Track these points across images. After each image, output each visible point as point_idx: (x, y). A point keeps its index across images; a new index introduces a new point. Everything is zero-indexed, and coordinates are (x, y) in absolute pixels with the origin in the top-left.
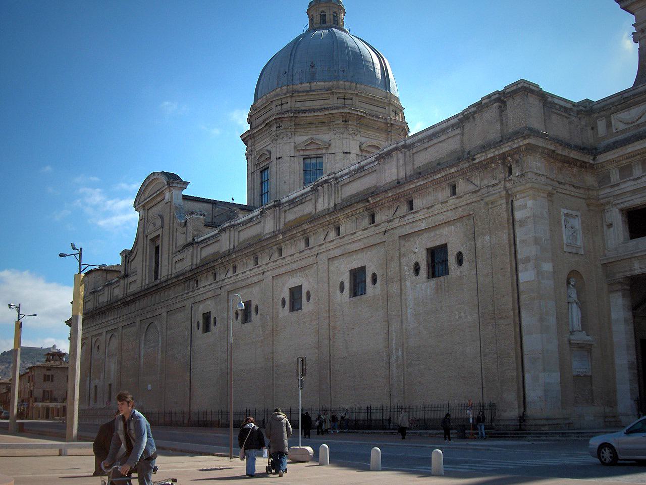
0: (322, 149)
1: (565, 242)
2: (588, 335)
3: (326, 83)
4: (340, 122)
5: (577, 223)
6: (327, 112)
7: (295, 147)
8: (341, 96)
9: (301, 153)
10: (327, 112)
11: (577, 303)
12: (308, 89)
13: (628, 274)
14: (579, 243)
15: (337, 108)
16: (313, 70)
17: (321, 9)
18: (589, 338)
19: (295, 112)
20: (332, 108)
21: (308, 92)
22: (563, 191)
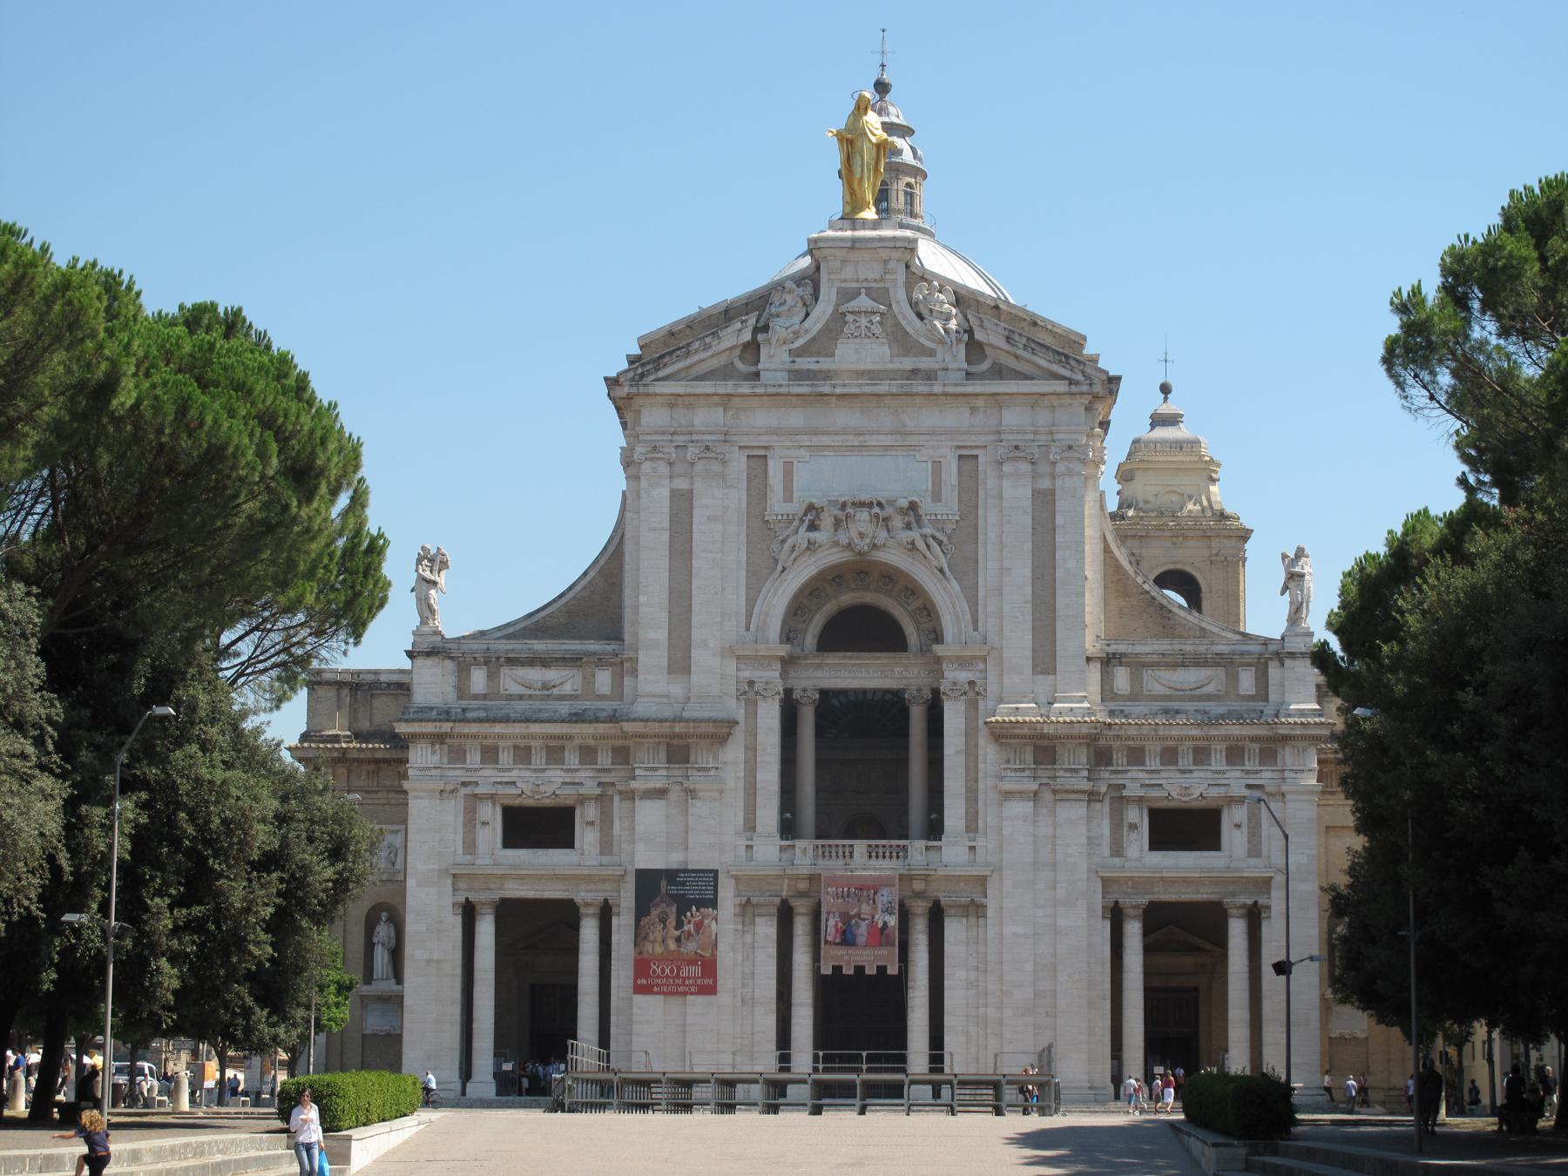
11: (383, 945)
22: (376, 802)
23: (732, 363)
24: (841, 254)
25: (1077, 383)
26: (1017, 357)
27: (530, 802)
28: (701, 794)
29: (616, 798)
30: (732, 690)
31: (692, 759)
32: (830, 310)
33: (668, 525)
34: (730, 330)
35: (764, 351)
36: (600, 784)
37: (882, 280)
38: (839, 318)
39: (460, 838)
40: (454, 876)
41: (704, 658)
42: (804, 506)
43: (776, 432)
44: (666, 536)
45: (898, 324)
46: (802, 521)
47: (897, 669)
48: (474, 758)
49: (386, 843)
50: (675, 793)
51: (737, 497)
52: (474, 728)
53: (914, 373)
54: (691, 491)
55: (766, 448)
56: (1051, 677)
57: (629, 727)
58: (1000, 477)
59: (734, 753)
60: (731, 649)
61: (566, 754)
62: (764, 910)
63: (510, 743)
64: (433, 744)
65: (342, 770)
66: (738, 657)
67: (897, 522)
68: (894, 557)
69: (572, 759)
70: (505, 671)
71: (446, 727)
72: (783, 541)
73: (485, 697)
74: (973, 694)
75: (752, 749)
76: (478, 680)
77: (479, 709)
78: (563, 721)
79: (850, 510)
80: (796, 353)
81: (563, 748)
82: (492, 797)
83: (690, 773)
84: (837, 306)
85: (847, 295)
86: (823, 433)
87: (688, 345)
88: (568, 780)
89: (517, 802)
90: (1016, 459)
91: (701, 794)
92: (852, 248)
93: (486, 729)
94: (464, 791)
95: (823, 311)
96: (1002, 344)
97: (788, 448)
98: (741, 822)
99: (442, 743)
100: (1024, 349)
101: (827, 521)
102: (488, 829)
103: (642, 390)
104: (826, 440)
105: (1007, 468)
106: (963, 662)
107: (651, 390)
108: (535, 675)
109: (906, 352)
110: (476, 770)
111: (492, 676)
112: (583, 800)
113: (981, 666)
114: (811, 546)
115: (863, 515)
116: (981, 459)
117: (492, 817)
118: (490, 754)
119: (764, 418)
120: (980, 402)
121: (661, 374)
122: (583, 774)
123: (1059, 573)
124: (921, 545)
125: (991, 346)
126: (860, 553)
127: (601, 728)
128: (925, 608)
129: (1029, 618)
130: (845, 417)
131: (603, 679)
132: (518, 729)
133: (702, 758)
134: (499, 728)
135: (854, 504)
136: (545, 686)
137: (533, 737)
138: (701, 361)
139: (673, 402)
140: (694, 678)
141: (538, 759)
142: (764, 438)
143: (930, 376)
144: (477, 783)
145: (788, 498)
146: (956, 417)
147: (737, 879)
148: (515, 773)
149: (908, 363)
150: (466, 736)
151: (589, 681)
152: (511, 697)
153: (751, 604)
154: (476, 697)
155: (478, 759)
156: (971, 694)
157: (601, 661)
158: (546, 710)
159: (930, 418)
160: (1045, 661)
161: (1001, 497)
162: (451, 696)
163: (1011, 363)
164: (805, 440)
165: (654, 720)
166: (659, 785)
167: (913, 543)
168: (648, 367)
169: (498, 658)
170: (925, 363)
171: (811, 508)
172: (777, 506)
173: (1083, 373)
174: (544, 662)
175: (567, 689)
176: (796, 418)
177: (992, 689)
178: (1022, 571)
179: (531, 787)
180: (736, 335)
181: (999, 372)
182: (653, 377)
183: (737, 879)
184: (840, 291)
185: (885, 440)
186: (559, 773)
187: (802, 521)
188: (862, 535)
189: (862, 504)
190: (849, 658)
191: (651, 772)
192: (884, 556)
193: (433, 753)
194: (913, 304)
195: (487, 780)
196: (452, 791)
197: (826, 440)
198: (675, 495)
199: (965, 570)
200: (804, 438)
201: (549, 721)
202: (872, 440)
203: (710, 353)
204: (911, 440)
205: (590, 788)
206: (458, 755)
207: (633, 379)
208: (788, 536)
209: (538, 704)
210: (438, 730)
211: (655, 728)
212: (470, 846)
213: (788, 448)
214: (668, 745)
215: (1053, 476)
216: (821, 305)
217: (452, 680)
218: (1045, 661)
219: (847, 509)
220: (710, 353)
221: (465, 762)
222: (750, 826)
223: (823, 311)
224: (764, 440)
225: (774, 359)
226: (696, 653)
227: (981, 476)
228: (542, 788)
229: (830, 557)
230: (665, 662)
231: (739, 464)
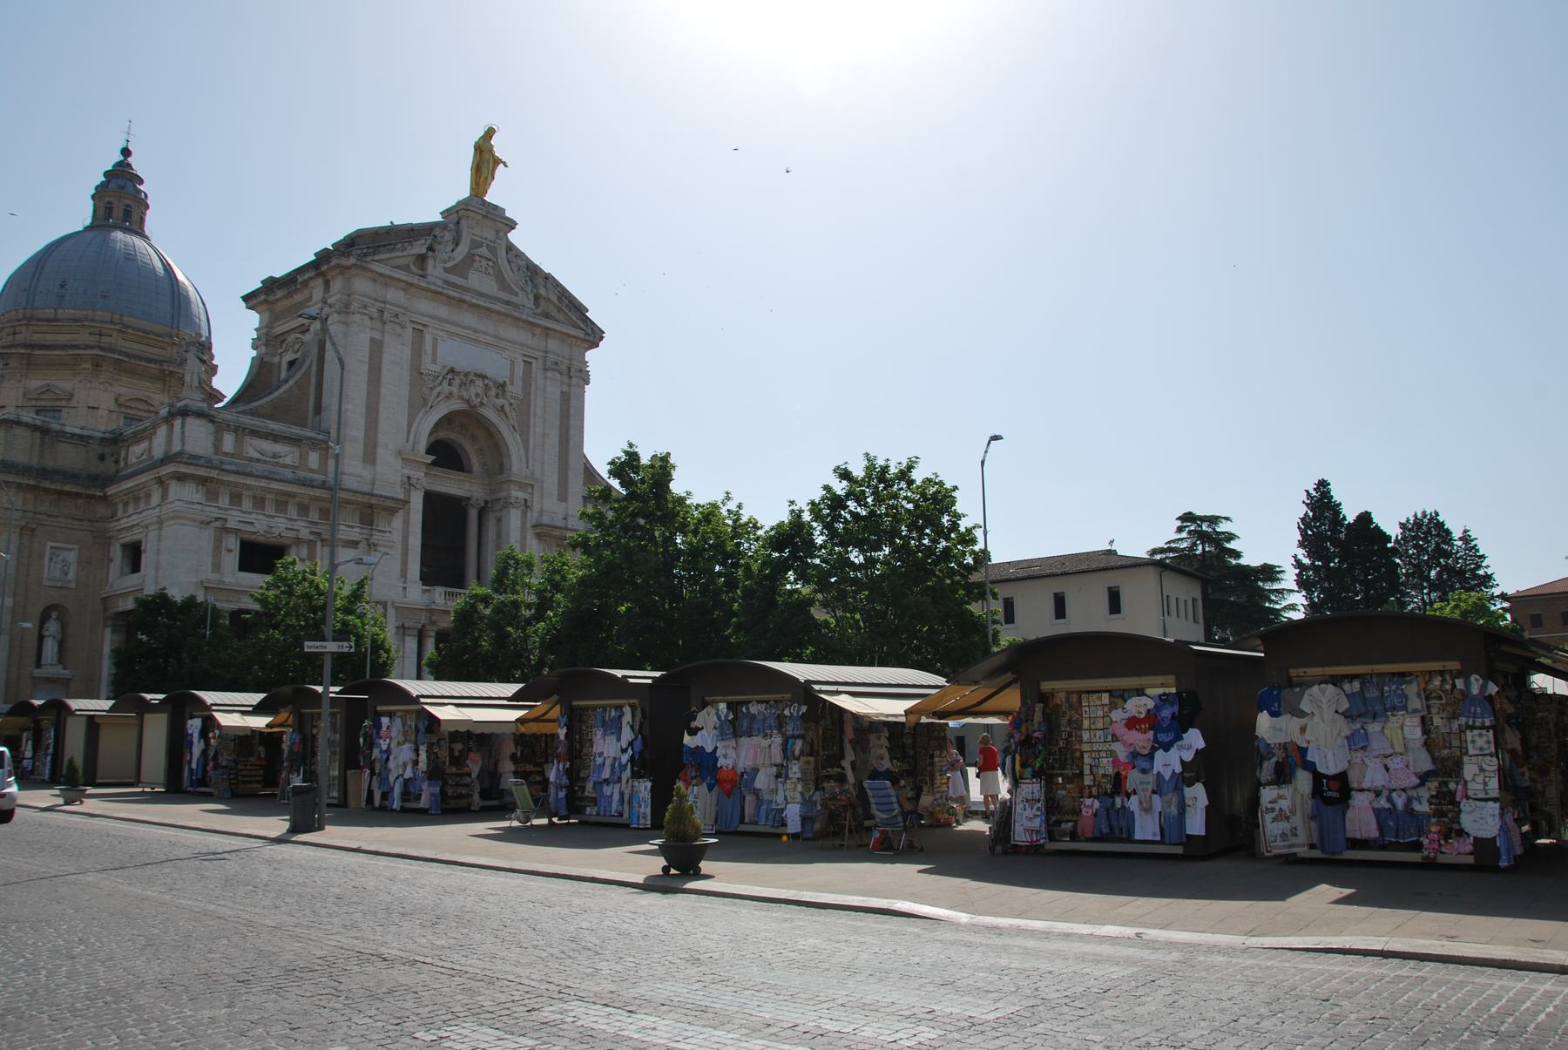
0: (61, 399)
1: (45, 575)
2: (65, 669)
3: (78, 312)
4: (88, 366)
5: (72, 557)
6: (70, 352)
7: (25, 395)
8: (96, 331)
9: (33, 403)
10: (70, 352)
12: (52, 317)
13: (116, 610)
14: (72, 575)
15: (87, 347)
16: (63, 291)
17: (108, 199)
18: (67, 672)
19: (25, 346)
20: (77, 347)
21: (49, 320)
23: (408, 265)
24: (479, 217)
25: (589, 335)
26: (560, 310)
27: (262, 539)
28: (379, 548)
29: (319, 544)
30: (398, 480)
31: (375, 524)
32: (466, 250)
33: (367, 360)
34: (419, 242)
35: (430, 263)
36: (311, 533)
37: (494, 242)
38: (470, 257)
39: (210, 560)
40: (206, 587)
41: (385, 455)
42: (447, 368)
43: (432, 317)
44: (366, 367)
45: (500, 271)
46: (444, 378)
47: (467, 485)
48: (224, 501)
49: (61, 558)
50: (362, 546)
51: (407, 353)
52: (231, 478)
53: (508, 303)
54: (382, 342)
55: (424, 325)
56: (564, 504)
57: (343, 495)
58: (545, 378)
59: (397, 522)
60: (400, 452)
61: (289, 508)
62: (410, 632)
63: (250, 493)
64: (198, 486)
65: (30, 496)
66: (403, 459)
67: (493, 393)
68: (489, 413)
69: (293, 513)
70: (248, 439)
71: (214, 474)
72: (432, 389)
73: (233, 456)
74: (526, 505)
75: (406, 522)
76: (229, 442)
77: (230, 464)
78: (290, 482)
79: (471, 377)
80: (447, 270)
81: (287, 502)
82: (236, 531)
83: (374, 532)
84: (470, 249)
85: (476, 245)
86: (458, 325)
87: (395, 244)
88: (289, 526)
89: (253, 537)
90: (554, 370)
91: (379, 548)
92: (484, 217)
93: (241, 480)
94: (218, 524)
95: (463, 248)
96: (554, 299)
97: (437, 329)
98: (399, 570)
99: (204, 485)
100: (567, 306)
101: (457, 382)
102: (232, 554)
103: (364, 265)
104: (459, 330)
105: (549, 374)
106: (522, 486)
107: (370, 266)
108: (268, 446)
109: (503, 290)
110: (226, 509)
111: (239, 442)
112: (298, 541)
113: (530, 491)
114: (449, 396)
115: (479, 383)
116: (534, 365)
117: (233, 543)
118: (236, 499)
119: (425, 306)
120: (538, 331)
121: (376, 258)
122: (299, 523)
123: (571, 442)
124: (507, 408)
125: (548, 300)
126: (474, 407)
127: (318, 493)
128: (481, 450)
129: (557, 466)
130: (469, 319)
131: (314, 458)
132: (263, 483)
133: (381, 523)
134: (249, 481)
135: (476, 374)
136: (275, 456)
137: (270, 491)
138: (398, 257)
139: (378, 278)
140: (378, 468)
141: (270, 510)
142: (425, 319)
143: (516, 306)
144: (226, 520)
145: (434, 361)
146: (524, 336)
147: (396, 608)
148: (253, 516)
149: (505, 296)
150: (221, 482)
151: (303, 458)
152: (251, 459)
153: (410, 426)
154: (226, 454)
155: (227, 501)
156: (523, 507)
157: (313, 444)
158: (278, 474)
159: (511, 333)
160: (563, 496)
161: (544, 391)
162: (211, 450)
163: (554, 312)
164: (447, 327)
165: (360, 493)
166: (356, 539)
167: (502, 407)
168: (371, 250)
169: (244, 429)
170: (514, 299)
171: (452, 370)
172: (427, 365)
173: (592, 329)
174: (275, 437)
175: (288, 460)
176: (443, 311)
177: (536, 506)
178: (554, 438)
179: (265, 528)
180: (419, 248)
181: (547, 316)
182: (370, 258)
183: (396, 608)
184: (473, 241)
185: (489, 339)
186: (285, 521)
187: (444, 378)
188: (477, 395)
189: (483, 377)
190: (445, 473)
191: (349, 529)
192: (486, 412)
193: (197, 492)
194: (509, 262)
195: (234, 518)
196: (209, 523)
197: (459, 330)
198: (373, 341)
199: (523, 429)
200: (448, 325)
201: (281, 481)
202: (482, 338)
203: (405, 254)
204: (503, 344)
205: (304, 533)
206: (212, 496)
207: (359, 255)
208: (435, 387)
209: (270, 468)
210: (206, 474)
211: (360, 498)
212: (217, 567)
213: (437, 329)
214: (361, 513)
215: (570, 385)
216: (459, 249)
217: (212, 438)
218: (563, 496)
219: (468, 378)
220: (405, 254)
221: (217, 502)
222: (404, 574)
223: (463, 248)
224: (425, 320)
225: (435, 270)
226: (380, 451)
227: (533, 375)
228: (273, 530)
229: (456, 405)
230: (361, 452)
231: (409, 332)
